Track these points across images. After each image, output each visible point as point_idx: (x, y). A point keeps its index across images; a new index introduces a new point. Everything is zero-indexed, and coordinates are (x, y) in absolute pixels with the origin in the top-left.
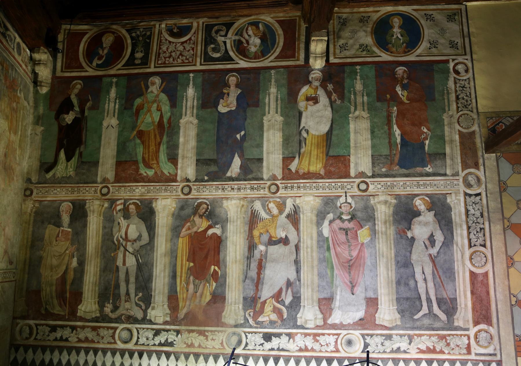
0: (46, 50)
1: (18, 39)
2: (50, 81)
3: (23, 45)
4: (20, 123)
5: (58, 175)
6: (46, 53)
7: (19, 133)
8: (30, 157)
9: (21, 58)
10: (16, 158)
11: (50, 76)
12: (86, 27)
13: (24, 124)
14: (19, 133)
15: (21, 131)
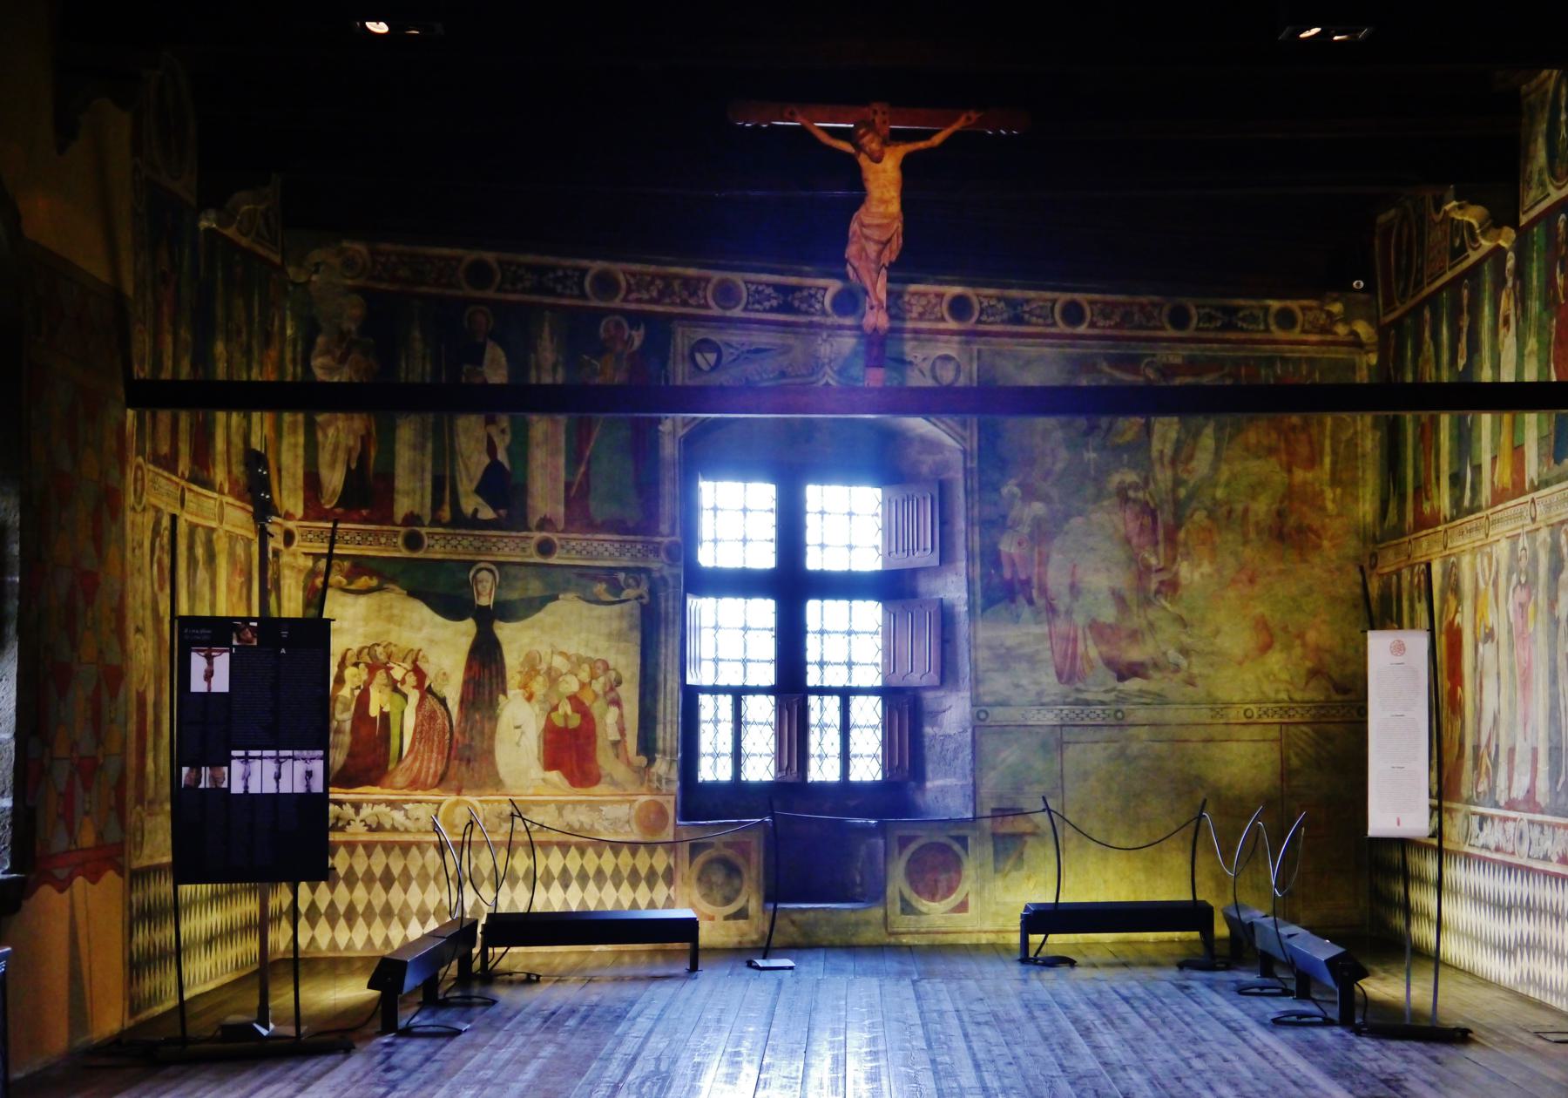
0: (1335, 295)
1: (1275, 304)
2: (1375, 339)
3: (1293, 304)
4: (1327, 443)
5: (1391, 524)
6: (1335, 300)
7: (1327, 460)
8: (1373, 494)
9: (1298, 329)
10: (1323, 509)
11: (1372, 331)
12: (1392, 213)
13: (1345, 436)
14: (1327, 460)
15: (1334, 452)
